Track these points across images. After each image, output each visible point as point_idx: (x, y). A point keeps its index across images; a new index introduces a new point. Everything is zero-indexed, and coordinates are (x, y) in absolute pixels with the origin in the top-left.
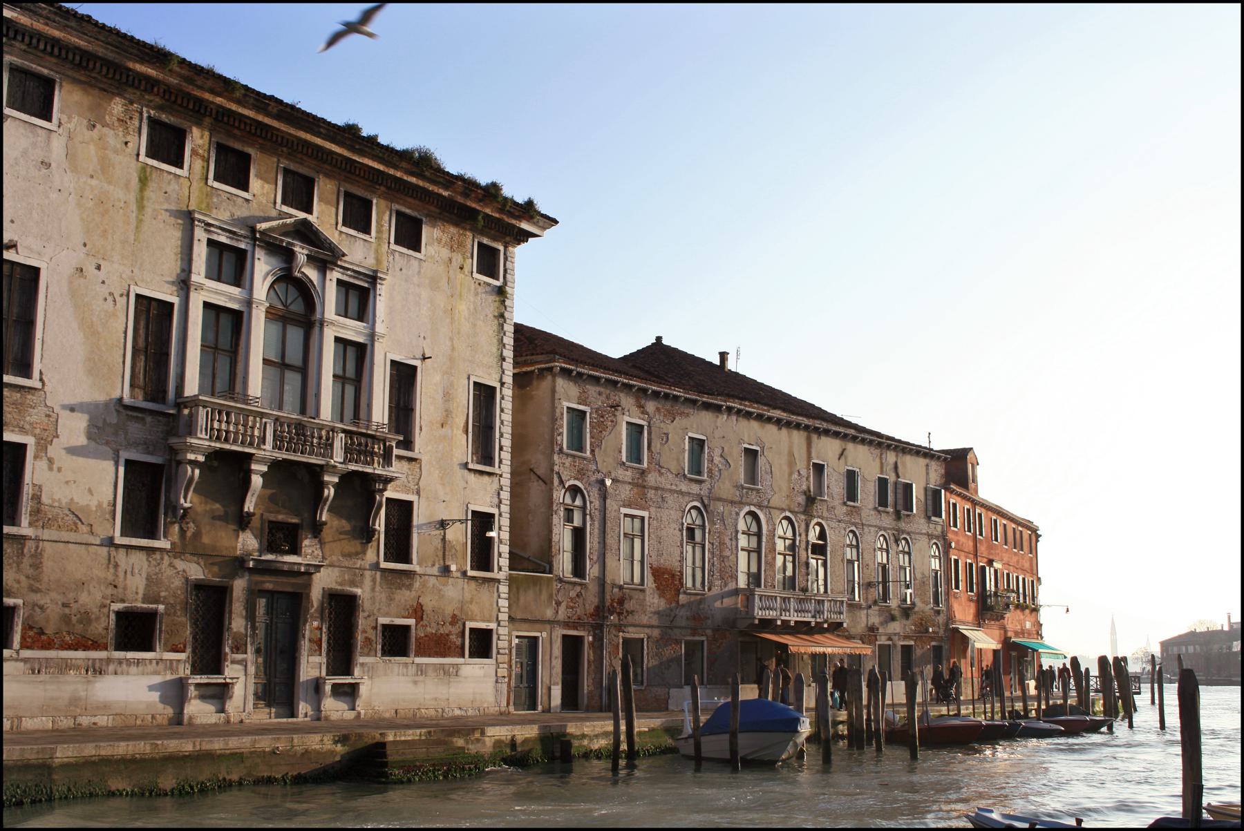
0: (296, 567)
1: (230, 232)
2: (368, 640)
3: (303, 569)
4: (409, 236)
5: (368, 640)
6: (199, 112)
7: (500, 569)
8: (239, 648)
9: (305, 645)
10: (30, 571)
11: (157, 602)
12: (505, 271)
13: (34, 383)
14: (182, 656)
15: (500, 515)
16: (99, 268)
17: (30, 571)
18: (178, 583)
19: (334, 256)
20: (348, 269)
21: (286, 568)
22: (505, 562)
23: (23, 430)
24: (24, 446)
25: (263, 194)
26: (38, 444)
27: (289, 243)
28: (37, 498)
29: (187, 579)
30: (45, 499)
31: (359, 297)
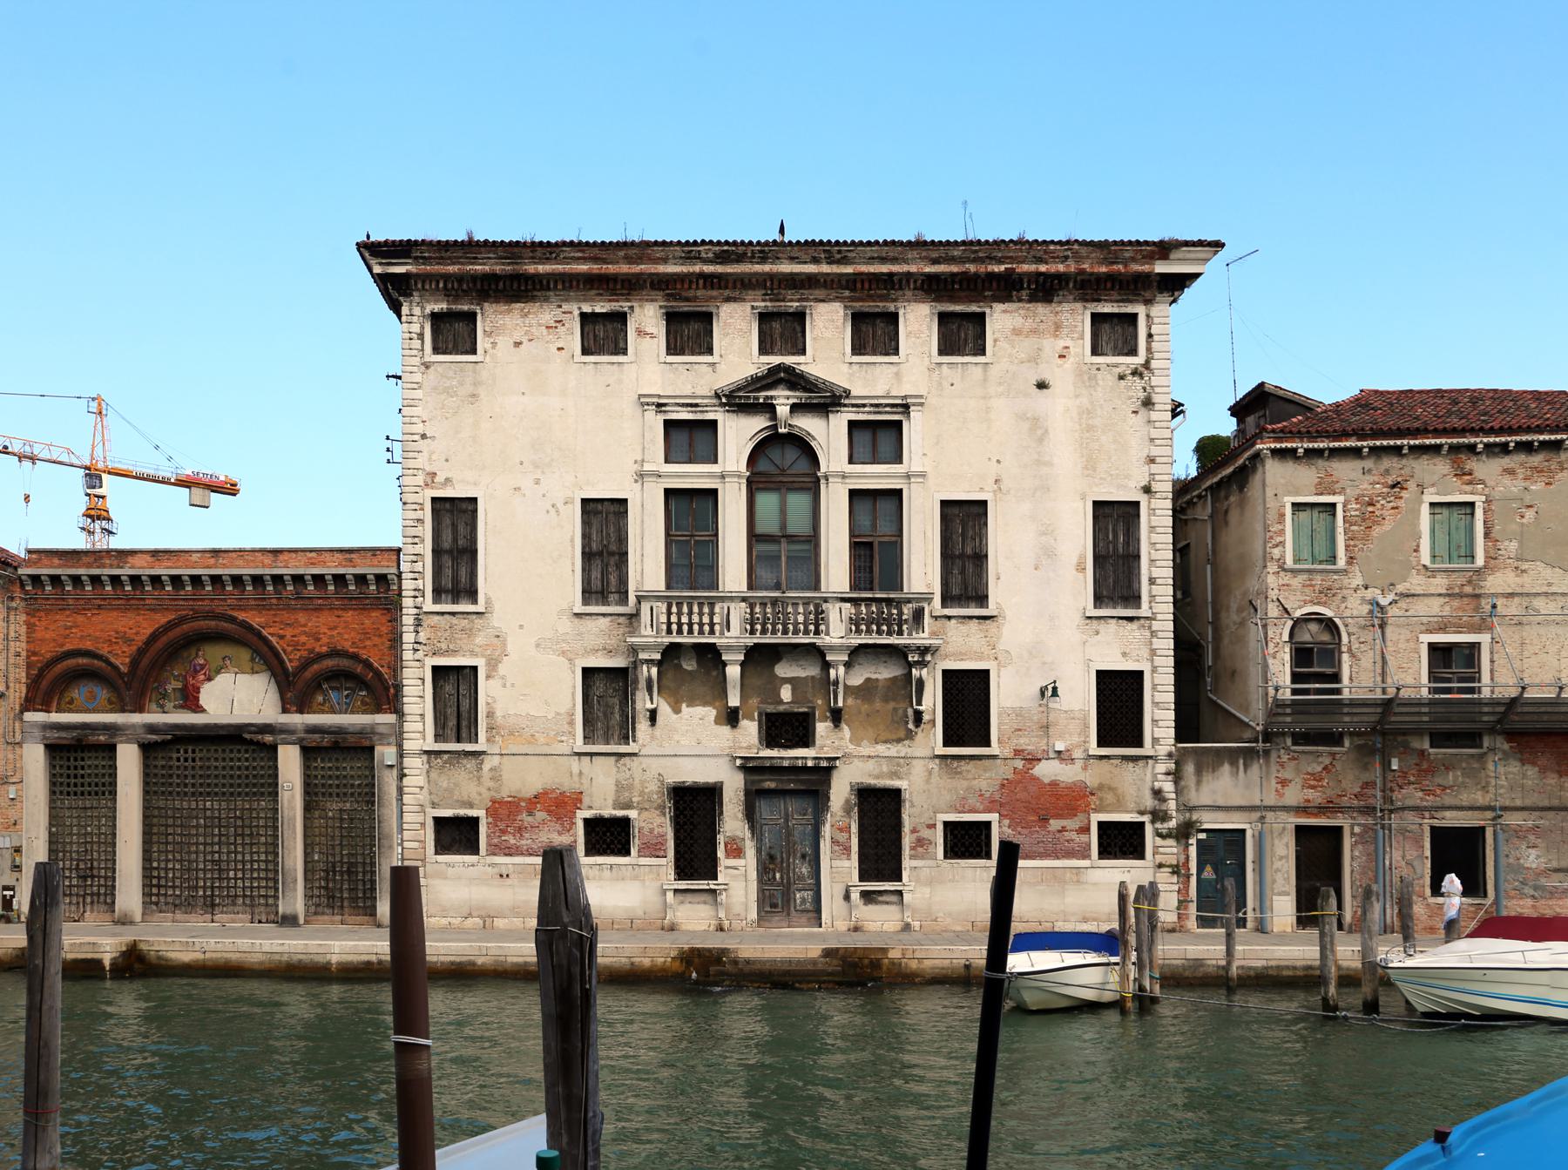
0: (800, 763)
1: (691, 405)
2: (920, 842)
3: (810, 764)
4: (961, 336)
5: (920, 842)
6: (630, 286)
7: (1155, 741)
8: (736, 851)
9: (825, 847)
10: (491, 784)
11: (628, 806)
12: (1150, 336)
13: (480, 608)
14: (663, 861)
15: (1154, 670)
16: (537, 482)
17: (491, 784)
18: (653, 787)
19: (834, 396)
20: (864, 406)
21: (786, 764)
22: (1167, 732)
23: (473, 654)
24: (475, 669)
25: (737, 347)
26: (488, 664)
27: (767, 398)
28: (490, 715)
29: (662, 782)
30: (499, 714)
31: (879, 435)
